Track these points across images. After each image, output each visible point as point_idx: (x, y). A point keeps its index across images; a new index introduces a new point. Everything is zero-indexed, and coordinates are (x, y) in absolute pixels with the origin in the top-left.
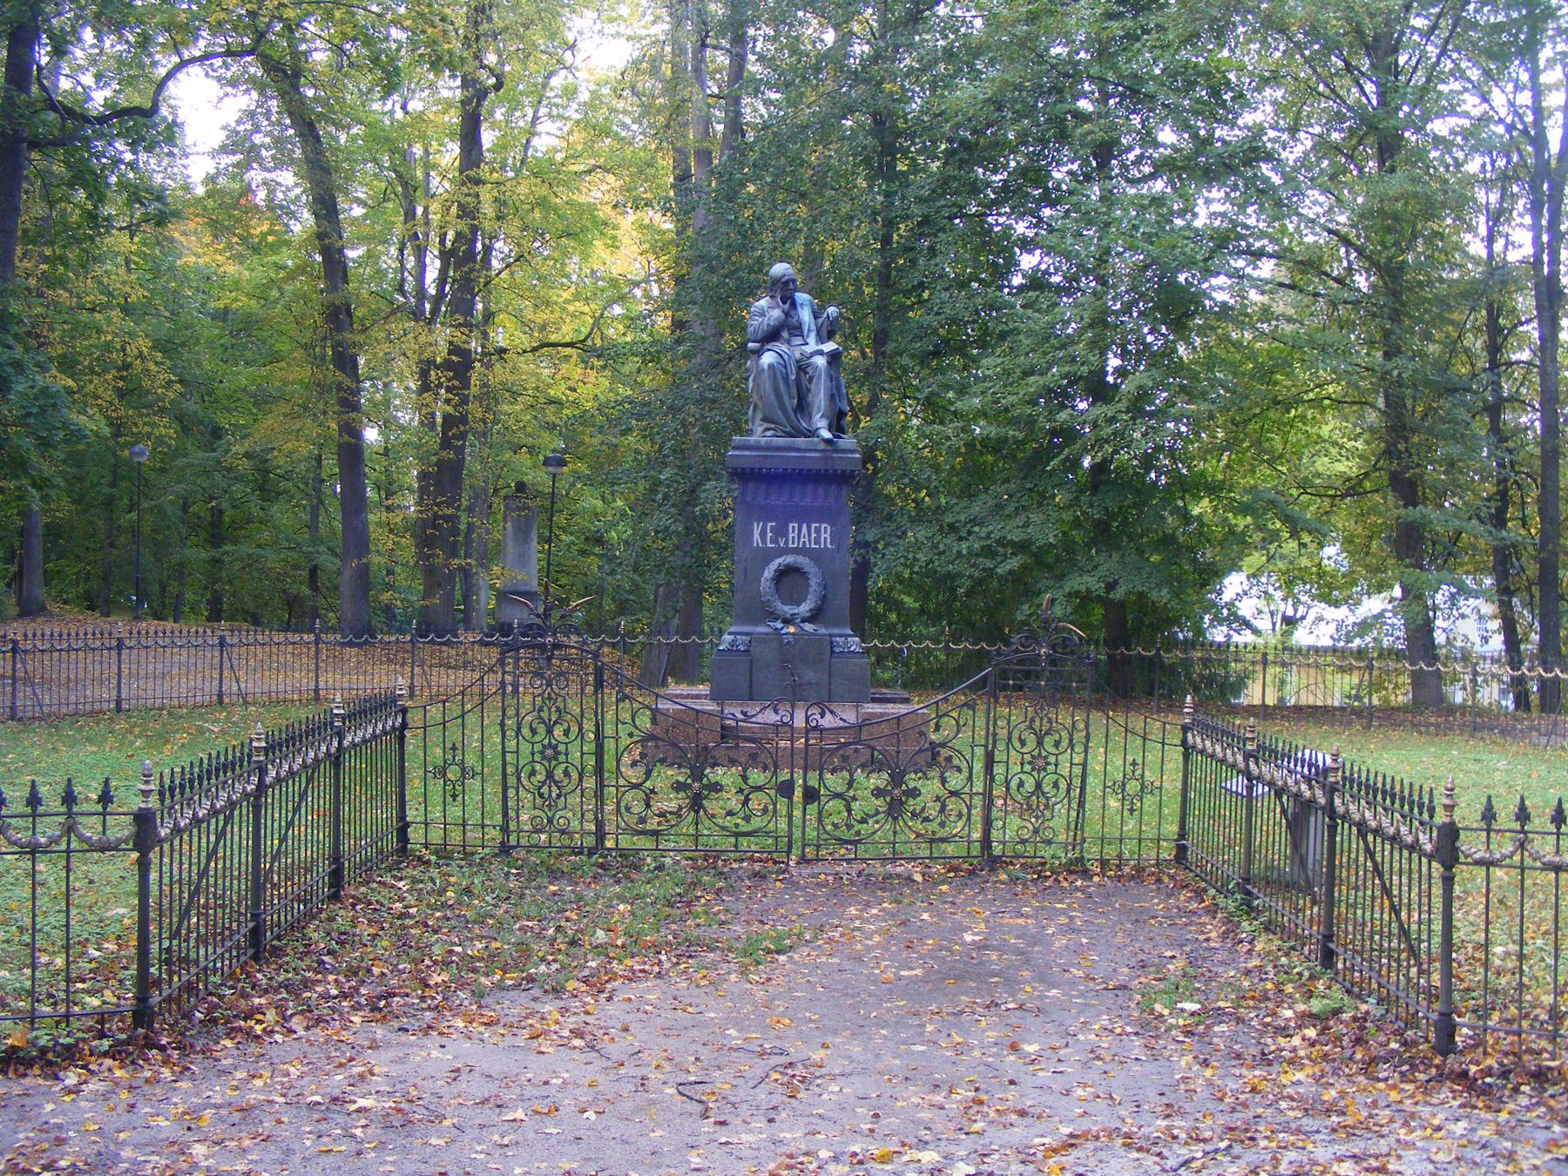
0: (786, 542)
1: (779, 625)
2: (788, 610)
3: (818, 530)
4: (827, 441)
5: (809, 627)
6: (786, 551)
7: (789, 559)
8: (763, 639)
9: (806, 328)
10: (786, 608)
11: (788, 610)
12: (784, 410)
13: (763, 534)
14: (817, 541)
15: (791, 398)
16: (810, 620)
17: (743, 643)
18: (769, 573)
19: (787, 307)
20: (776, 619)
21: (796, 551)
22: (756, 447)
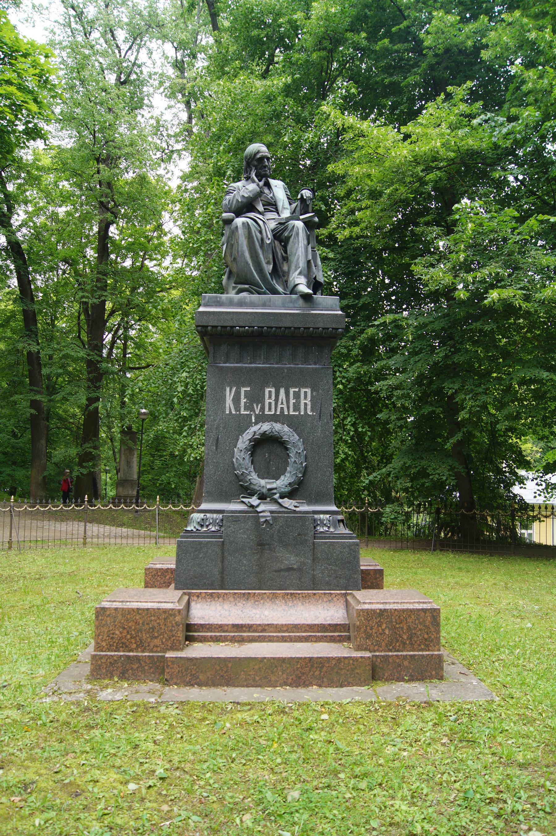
0: (263, 409)
1: (254, 501)
2: (264, 484)
3: (297, 396)
4: (306, 297)
5: (287, 503)
6: (262, 418)
7: (266, 427)
8: (234, 517)
9: (280, 205)
10: (263, 482)
11: (264, 484)
12: (260, 270)
13: (236, 400)
14: (297, 407)
15: (268, 263)
16: (291, 495)
17: (214, 523)
18: (244, 441)
19: (261, 184)
20: (252, 495)
21: (274, 418)
22: (231, 303)
